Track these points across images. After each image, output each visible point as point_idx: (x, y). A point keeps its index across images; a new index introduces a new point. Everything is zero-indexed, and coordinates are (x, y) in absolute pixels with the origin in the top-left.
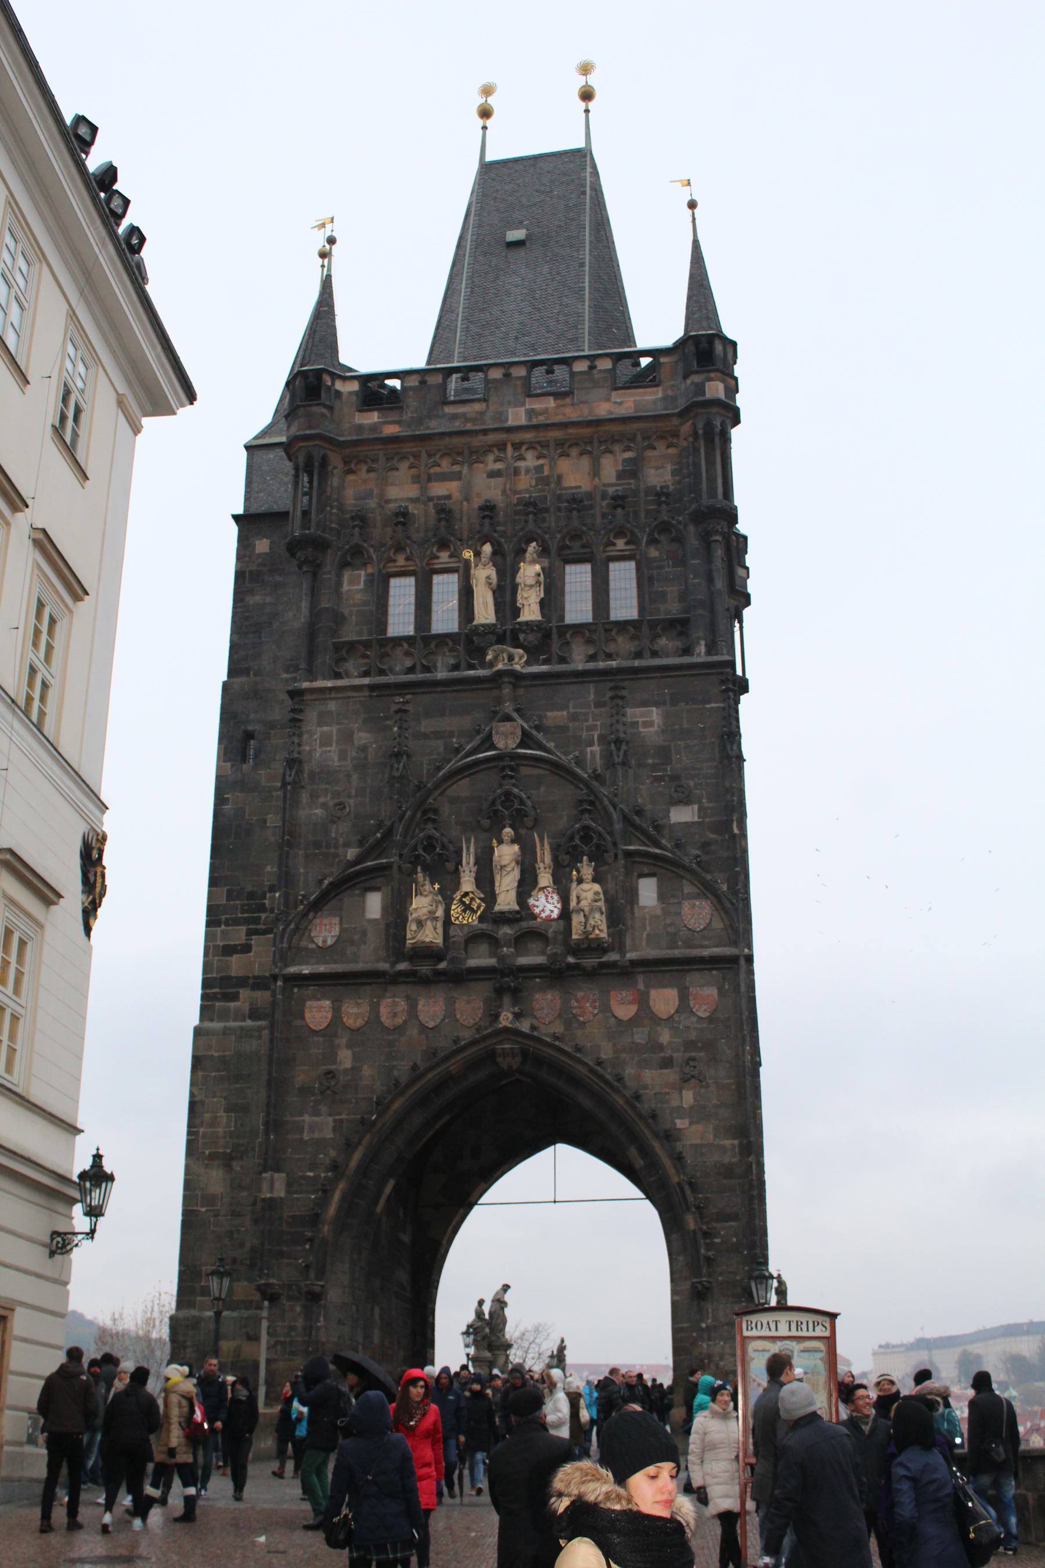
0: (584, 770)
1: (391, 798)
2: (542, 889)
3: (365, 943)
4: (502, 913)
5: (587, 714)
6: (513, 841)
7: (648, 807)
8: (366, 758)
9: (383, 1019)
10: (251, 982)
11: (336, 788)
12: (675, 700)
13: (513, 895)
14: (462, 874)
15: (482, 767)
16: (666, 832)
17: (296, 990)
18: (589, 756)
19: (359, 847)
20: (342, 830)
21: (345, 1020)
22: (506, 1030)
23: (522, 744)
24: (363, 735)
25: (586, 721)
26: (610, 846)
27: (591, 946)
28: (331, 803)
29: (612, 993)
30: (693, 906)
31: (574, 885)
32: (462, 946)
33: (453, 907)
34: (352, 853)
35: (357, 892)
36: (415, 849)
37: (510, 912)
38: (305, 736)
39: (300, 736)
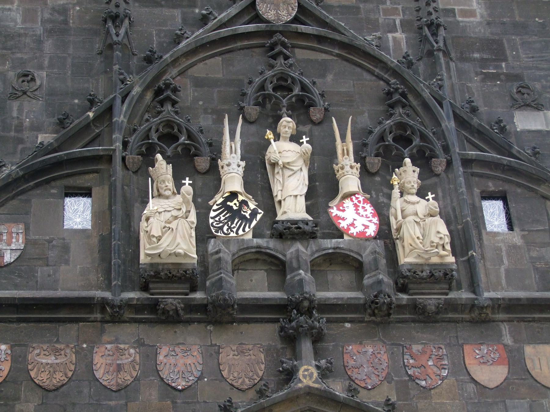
3: (67, 262)
8: (66, 22)
9: (98, 375)
11: (19, 55)
13: (302, 202)
15: (239, 44)
18: (391, 44)
19: (56, 132)
21: (33, 374)
22: (309, 392)
23: (296, 20)
26: (439, 150)
29: (467, 348)
31: (396, 192)
33: (212, 214)
34: (45, 138)
35: (54, 191)
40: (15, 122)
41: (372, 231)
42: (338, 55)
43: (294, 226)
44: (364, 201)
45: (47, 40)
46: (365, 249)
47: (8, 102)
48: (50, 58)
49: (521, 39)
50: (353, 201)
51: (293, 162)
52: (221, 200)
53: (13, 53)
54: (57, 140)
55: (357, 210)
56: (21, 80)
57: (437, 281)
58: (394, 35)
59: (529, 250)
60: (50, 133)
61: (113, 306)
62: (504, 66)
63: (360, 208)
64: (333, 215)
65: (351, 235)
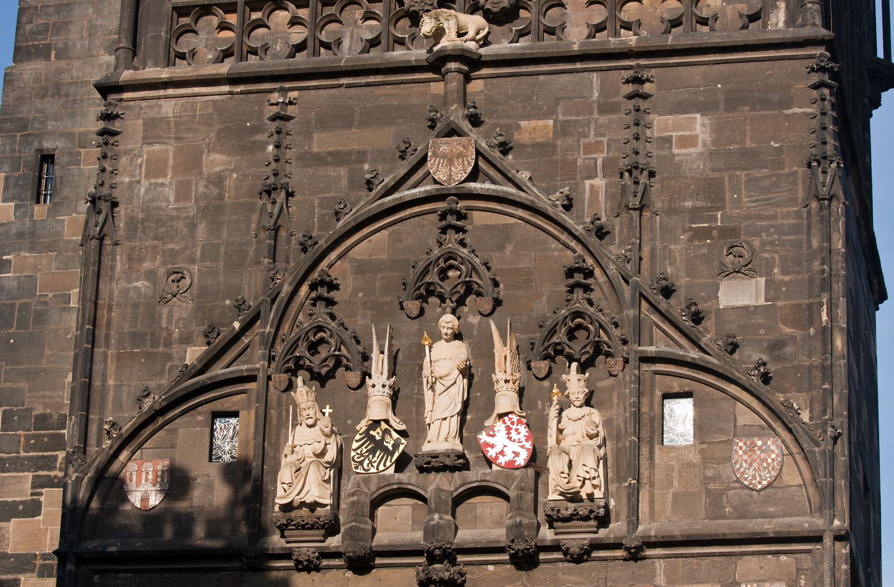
0: (579, 219)
1: (259, 263)
2: (501, 416)
4: (435, 456)
5: (588, 124)
6: (457, 336)
7: (682, 282)
8: (221, 196)
10: (39, 562)
11: (171, 246)
12: (733, 101)
14: (370, 390)
16: (709, 323)
17: (96, 578)
18: (587, 195)
20: (179, 313)
23: (473, 176)
24: (217, 157)
25: (586, 135)
27: (580, 510)
28: (162, 271)
30: (751, 448)
32: (367, 510)
33: (355, 445)
34: (193, 354)
35: (200, 418)
36: (295, 345)
37: (447, 455)
38: (124, 160)
39: (116, 158)
40: (164, 334)
41: (522, 459)
42: (521, 218)
43: (434, 460)
44: (519, 422)
45: (201, 223)
46: (513, 481)
47: (158, 308)
48: (203, 248)
49: (746, 175)
50: (504, 422)
51: (446, 376)
52: (364, 428)
53: (164, 244)
54: (199, 360)
55: (508, 433)
56: (172, 277)
57: (586, 518)
58: (592, 182)
59: (705, 467)
60: (199, 346)
61: (248, 558)
62: (719, 216)
63: (513, 431)
64: (482, 441)
65: (499, 465)
